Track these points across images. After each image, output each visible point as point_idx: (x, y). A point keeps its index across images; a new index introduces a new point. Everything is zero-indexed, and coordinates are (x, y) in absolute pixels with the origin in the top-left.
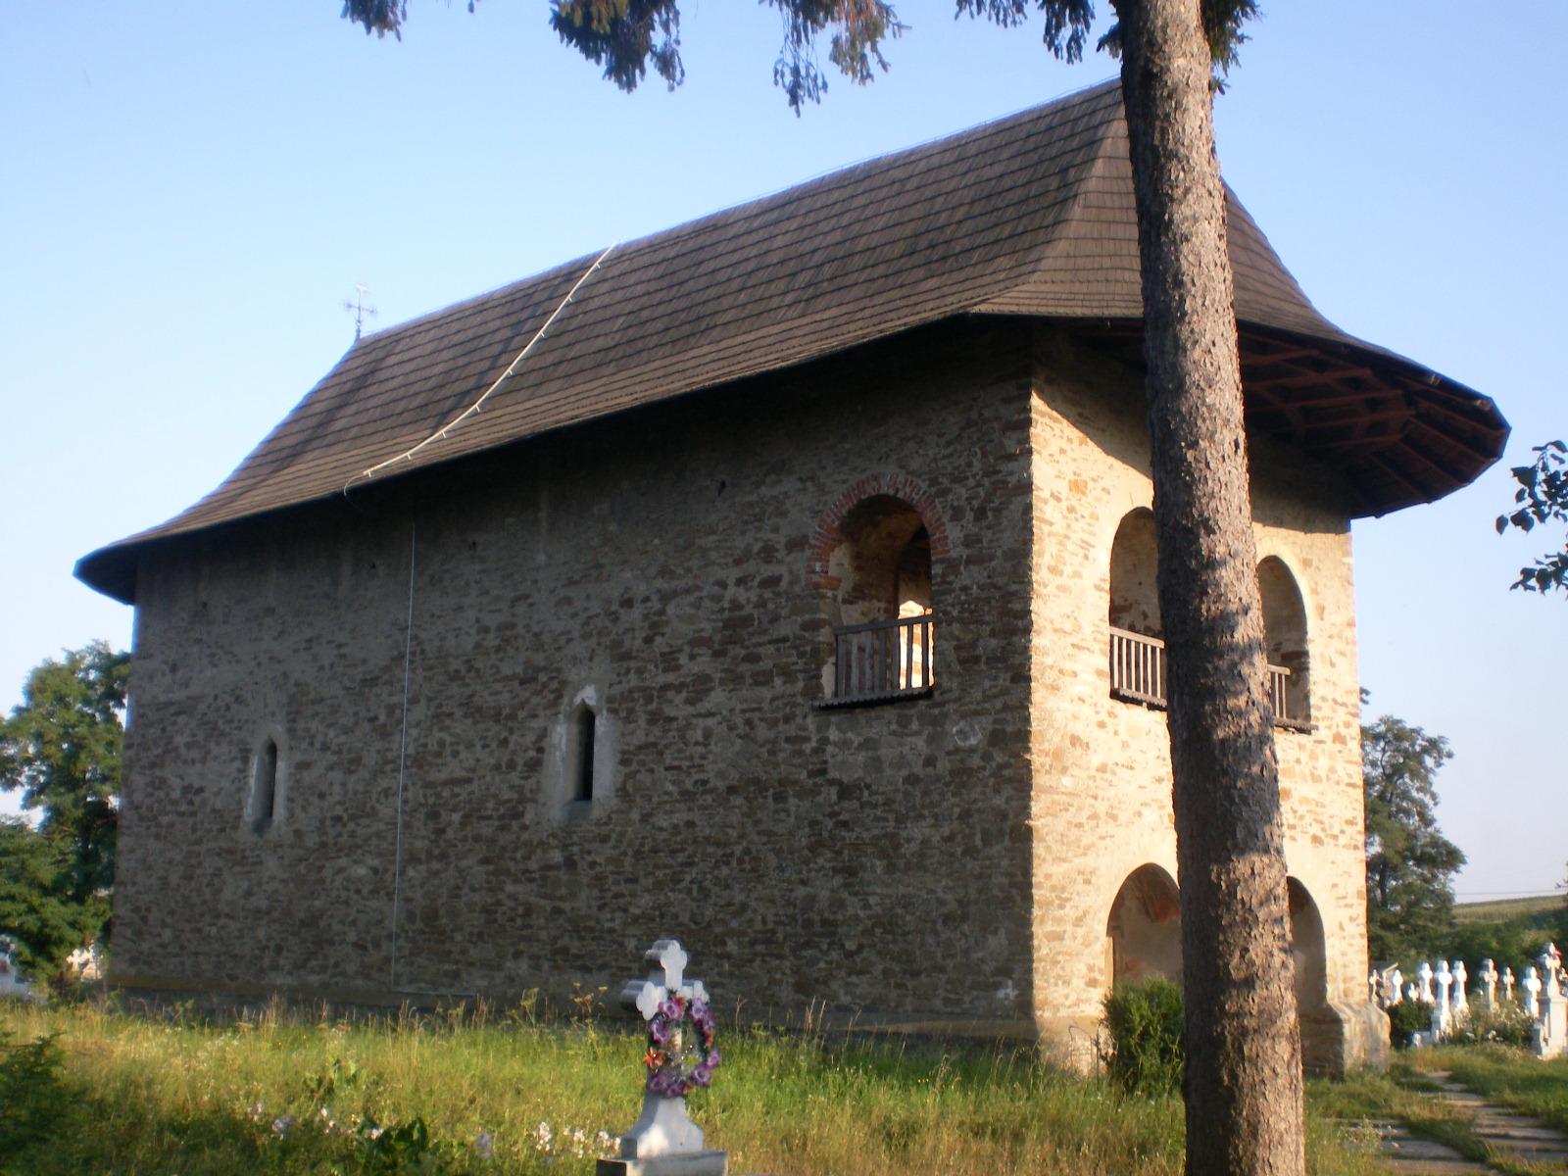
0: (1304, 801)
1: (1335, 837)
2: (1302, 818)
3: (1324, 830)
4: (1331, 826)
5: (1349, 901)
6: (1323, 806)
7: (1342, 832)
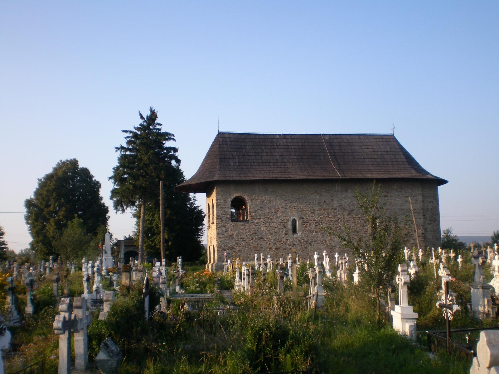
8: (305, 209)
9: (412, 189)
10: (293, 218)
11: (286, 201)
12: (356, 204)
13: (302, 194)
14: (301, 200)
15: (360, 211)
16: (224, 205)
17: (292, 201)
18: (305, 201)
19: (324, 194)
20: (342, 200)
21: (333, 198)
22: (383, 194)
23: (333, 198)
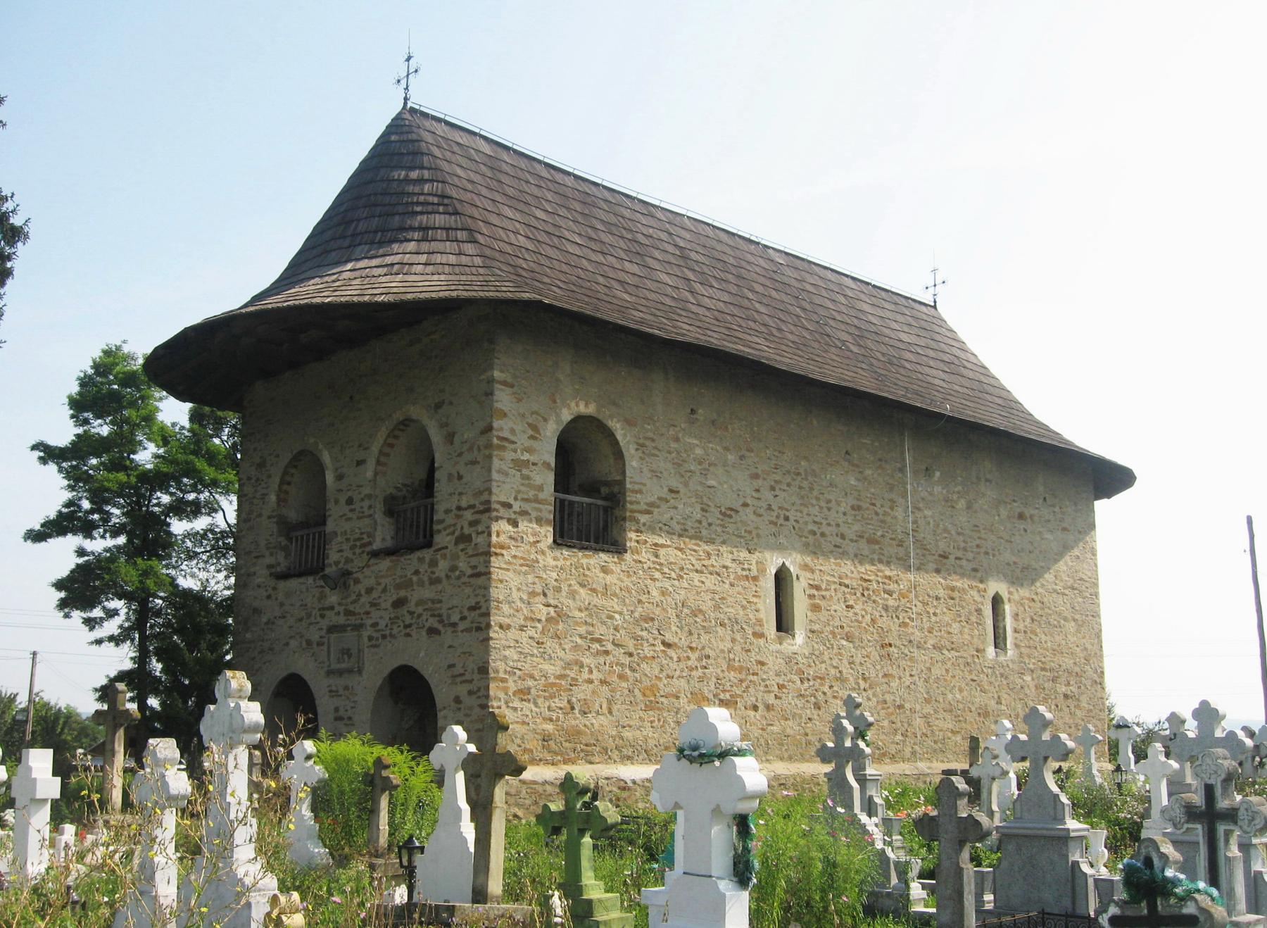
1: (454, 625)
2: (419, 616)
3: (441, 621)
4: (449, 616)
5: (467, 677)
6: (440, 601)
7: (463, 618)
8: (815, 528)
9: (1076, 504)
10: (780, 562)
11: (756, 476)
13: (805, 458)
15: (964, 563)
16: (528, 450)
18: (815, 493)
19: (868, 472)
20: (919, 509)
21: (893, 496)
23: (893, 496)
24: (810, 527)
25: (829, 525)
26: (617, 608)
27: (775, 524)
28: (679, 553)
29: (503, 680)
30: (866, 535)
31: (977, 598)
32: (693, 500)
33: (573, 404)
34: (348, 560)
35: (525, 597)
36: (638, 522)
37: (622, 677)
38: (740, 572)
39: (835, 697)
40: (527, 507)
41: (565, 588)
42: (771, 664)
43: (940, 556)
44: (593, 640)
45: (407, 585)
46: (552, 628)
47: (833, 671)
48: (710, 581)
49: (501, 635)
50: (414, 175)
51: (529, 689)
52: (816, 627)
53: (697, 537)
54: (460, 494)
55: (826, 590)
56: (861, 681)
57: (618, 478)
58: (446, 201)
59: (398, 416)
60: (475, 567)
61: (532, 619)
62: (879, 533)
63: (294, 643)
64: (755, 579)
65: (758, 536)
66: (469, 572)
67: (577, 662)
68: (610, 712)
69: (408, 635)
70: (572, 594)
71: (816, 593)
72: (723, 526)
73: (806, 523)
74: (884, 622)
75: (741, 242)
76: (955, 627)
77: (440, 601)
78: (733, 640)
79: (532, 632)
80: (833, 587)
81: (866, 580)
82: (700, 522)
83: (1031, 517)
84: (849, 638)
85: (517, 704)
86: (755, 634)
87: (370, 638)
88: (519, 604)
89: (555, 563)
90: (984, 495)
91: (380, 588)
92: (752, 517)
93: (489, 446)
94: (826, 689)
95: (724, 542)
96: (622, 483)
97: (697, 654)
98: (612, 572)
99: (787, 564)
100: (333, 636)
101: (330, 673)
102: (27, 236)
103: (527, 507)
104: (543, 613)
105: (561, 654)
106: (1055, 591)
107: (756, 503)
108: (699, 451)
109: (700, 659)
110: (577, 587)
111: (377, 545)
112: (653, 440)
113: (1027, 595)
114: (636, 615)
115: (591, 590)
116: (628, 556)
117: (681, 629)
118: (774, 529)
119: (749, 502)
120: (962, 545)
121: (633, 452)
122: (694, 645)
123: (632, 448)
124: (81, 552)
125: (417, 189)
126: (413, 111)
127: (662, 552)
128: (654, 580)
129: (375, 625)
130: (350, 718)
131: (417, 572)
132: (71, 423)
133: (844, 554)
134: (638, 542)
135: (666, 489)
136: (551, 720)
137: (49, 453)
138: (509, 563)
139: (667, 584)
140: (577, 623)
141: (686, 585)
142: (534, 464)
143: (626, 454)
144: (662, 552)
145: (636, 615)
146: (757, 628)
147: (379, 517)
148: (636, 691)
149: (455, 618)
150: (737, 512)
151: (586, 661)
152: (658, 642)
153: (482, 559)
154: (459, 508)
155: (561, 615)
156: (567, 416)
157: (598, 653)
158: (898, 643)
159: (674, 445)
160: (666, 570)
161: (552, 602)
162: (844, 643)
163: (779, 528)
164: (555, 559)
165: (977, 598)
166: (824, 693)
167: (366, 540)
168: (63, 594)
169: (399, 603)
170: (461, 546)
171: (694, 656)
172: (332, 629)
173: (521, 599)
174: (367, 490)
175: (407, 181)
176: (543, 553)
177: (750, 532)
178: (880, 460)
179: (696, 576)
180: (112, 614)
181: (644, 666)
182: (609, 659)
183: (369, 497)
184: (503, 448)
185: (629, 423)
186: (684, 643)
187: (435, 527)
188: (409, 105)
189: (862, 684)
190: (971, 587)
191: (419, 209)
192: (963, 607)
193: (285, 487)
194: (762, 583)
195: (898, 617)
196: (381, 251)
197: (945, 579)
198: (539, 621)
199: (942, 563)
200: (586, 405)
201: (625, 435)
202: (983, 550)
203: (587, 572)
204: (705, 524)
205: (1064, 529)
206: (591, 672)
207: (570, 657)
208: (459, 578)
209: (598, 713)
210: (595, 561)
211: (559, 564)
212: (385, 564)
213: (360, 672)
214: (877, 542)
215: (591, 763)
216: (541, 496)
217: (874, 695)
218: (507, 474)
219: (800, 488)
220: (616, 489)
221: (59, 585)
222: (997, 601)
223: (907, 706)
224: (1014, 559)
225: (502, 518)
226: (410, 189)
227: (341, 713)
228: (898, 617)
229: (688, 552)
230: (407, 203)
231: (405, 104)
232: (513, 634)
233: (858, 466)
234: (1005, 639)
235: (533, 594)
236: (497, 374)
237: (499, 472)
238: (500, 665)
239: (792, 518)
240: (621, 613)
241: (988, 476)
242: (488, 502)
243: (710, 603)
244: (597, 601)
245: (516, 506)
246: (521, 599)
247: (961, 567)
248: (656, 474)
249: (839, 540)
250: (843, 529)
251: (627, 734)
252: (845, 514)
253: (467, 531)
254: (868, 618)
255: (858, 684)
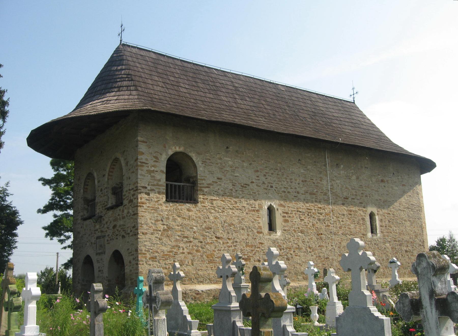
0: (120, 226)
1: (129, 234)
3: (125, 233)
5: (133, 253)
6: (125, 225)
7: (131, 231)
8: (285, 190)
9: (408, 175)
10: (269, 203)
11: (257, 171)
12: (350, 189)
13: (280, 163)
14: (280, 173)
15: (356, 200)
17: (266, 173)
18: (285, 176)
19: (309, 167)
20: (334, 180)
21: (321, 176)
22: (380, 178)
23: (321, 176)
24: (283, 189)
25: (291, 188)
26: (194, 224)
27: (266, 189)
28: (223, 203)
29: (144, 254)
30: (309, 192)
31: (362, 214)
32: (229, 182)
33: (173, 148)
34: (101, 212)
35: (153, 222)
36: (203, 191)
37: (197, 251)
38: (251, 208)
39: (296, 255)
40: (153, 188)
41: (171, 218)
42: (266, 244)
43: (344, 198)
44: (184, 237)
45: (116, 220)
46: (166, 233)
47: (295, 245)
48: (237, 213)
49: (143, 236)
50: (119, 68)
51: (156, 257)
52: (286, 228)
53: (231, 196)
54: (130, 184)
55: (291, 214)
56: (308, 249)
57: (195, 175)
58: (129, 76)
59: (113, 157)
60: (134, 212)
61: (157, 230)
62: (315, 191)
63: (88, 244)
64: (258, 211)
65: (259, 194)
66: (132, 213)
67: (177, 246)
68: (193, 265)
69: (117, 239)
70: (174, 220)
71: (286, 215)
72: (242, 191)
73: (281, 188)
74: (319, 225)
75: (266, 83)
76: (352, 226)
77: (125, 225)
78: (248, 235)
79: (157, 235)
80: (294, 212)
81: (309, 209)
82: (232, 190)
83: (387, 181)
84: (302, 232)
85: (151, 263)
86: (258, 232)
87: (107, 241)
88: (151, 225)
89: (166, 208)
90: (364, 173)
91: (109, 222)
92: (256, 187)
93: (137, 165)
94: (292, 252)
95: (243, 197)
96: (196, 177)
97: (231, 241)
98: (192, 211)
99: (272, 204)
100: (98, 240)
101: (97, 254)
102: (8, 105)
103: (153, 188)
104: (161, 227)
105: (170, 243)
106: (400, 210)
107: (258, 181)
108: (230, 163)
109: (233, 243)
110: (176, 217)
111: (110, 205)
112: (210, 160)
113: (386, 212)
114: (203, 227)
115: (183, 218)
116: (199, 205)
117: (224, 231)
118: (266, 191)
119: (254, 181)
120: (355, 193)
121: (200, 164)
122: (230, 237)
123: (200, 163)
124: (55, 216)
125: (119, 73)
126: (124, 45)
127: (214, 202)
128: (211, 213)
129: (108, 235)
130: (102, 271)
131: (119, 215)
132: (53, 170)
133: (299, 200)
134: (203, 199)
135: (216, 178)
136: (166, 268)
137: (46, 182)
138: (146, 209)
139: (217, 214)
140: (176, 231)
141: (226, 214)
142: (156, 171)
143: (197, 165)
144: (214, 202)
145: (203, 227)
146: (259, 230)
147: (110, 195)
148: (204, 256)
149: (129, 231)
150: (249, 185)
151: (181, 245)
152: (214, 237)
153: (135, 208)
154: (129, 190)
155: (169, 228)
156: (170, 153)
157: (186, 242)
158: (325, 233)
159: (219, 161)
160: (217, 209)
161: (165, 223)
162: (300, 234)
163: (268, 191)
164: (167, 207)
165: (362, 214)
166: (291, 254)
167: (106, 204)
168: (47, 231)
169: (114, 227)
170: (130, 204)
171: (230, 242)
172: (98, 238)
173: (152, 223)
174: (105, 186)
175: (117, 70)
176: (161, 205)
177: (255, 193)
178: (315, 162)
179: (230, 211)
180: (68, 237)
181: (207, 246)
182: (191, 244)
183: (106, 188)
184: (143, 166)
185: (199, 154)
186: (225, 236)
187: (124, 197)
188: (122, 43)
189: (309, 250)
190: (360, 210)
191: (118, 80)
192: (356, 218)
193: (86, 187)
194: (261, 212)
195: (325, 223)
196: (102, 97)
197: (347, 207)
198: (160, 231)
199: (345, 201)
200: (179, 148)
201: (197, 158)
202: (364, 195)
203: (181, 211)
204: (234, 190)
205: (403, 185)
206: (183, 249)
207: (174, 244)
208: (130, 216)
209: (187, 265)
210: (184, 207)
211: (168, 209)
212: (110, 212)
213: (105, 253)
214: (314, 194)
215: (184, 284)
216: (160, 183)
217: (314, 254)
218: (144, 176)
219: (278, 175)
220: (194, 179)
221: (45, 228)
222: (372, 216)
223: (330, 258)
224: (380, 198)
225: (142, 192)
226: (117, 73)
227: (100, 269)
228: (325, 223)
229: (226, 202)
230: (115, 78)
231: (121, 42)
232: (147, 236)
233: (304, 165)
234: (376, 230)
235: (157, 221)
236: (139, 138)
237: (141, 175)
238: (143, 248)
239: (274, 187)
240: (196, 227)
241: (366, 166)
242: (137, 187)
243: (237, 221)
244: (186, 222)
245: (149, 188)
246: (152, 223)
247: (354, 202)
248: (212, 173)
249: (296, 194)
250: (298, 189)
251: (200, 273)
252: (299, 184)
253: (132, 198)
254: (311, 224)
255: (307, 250)
